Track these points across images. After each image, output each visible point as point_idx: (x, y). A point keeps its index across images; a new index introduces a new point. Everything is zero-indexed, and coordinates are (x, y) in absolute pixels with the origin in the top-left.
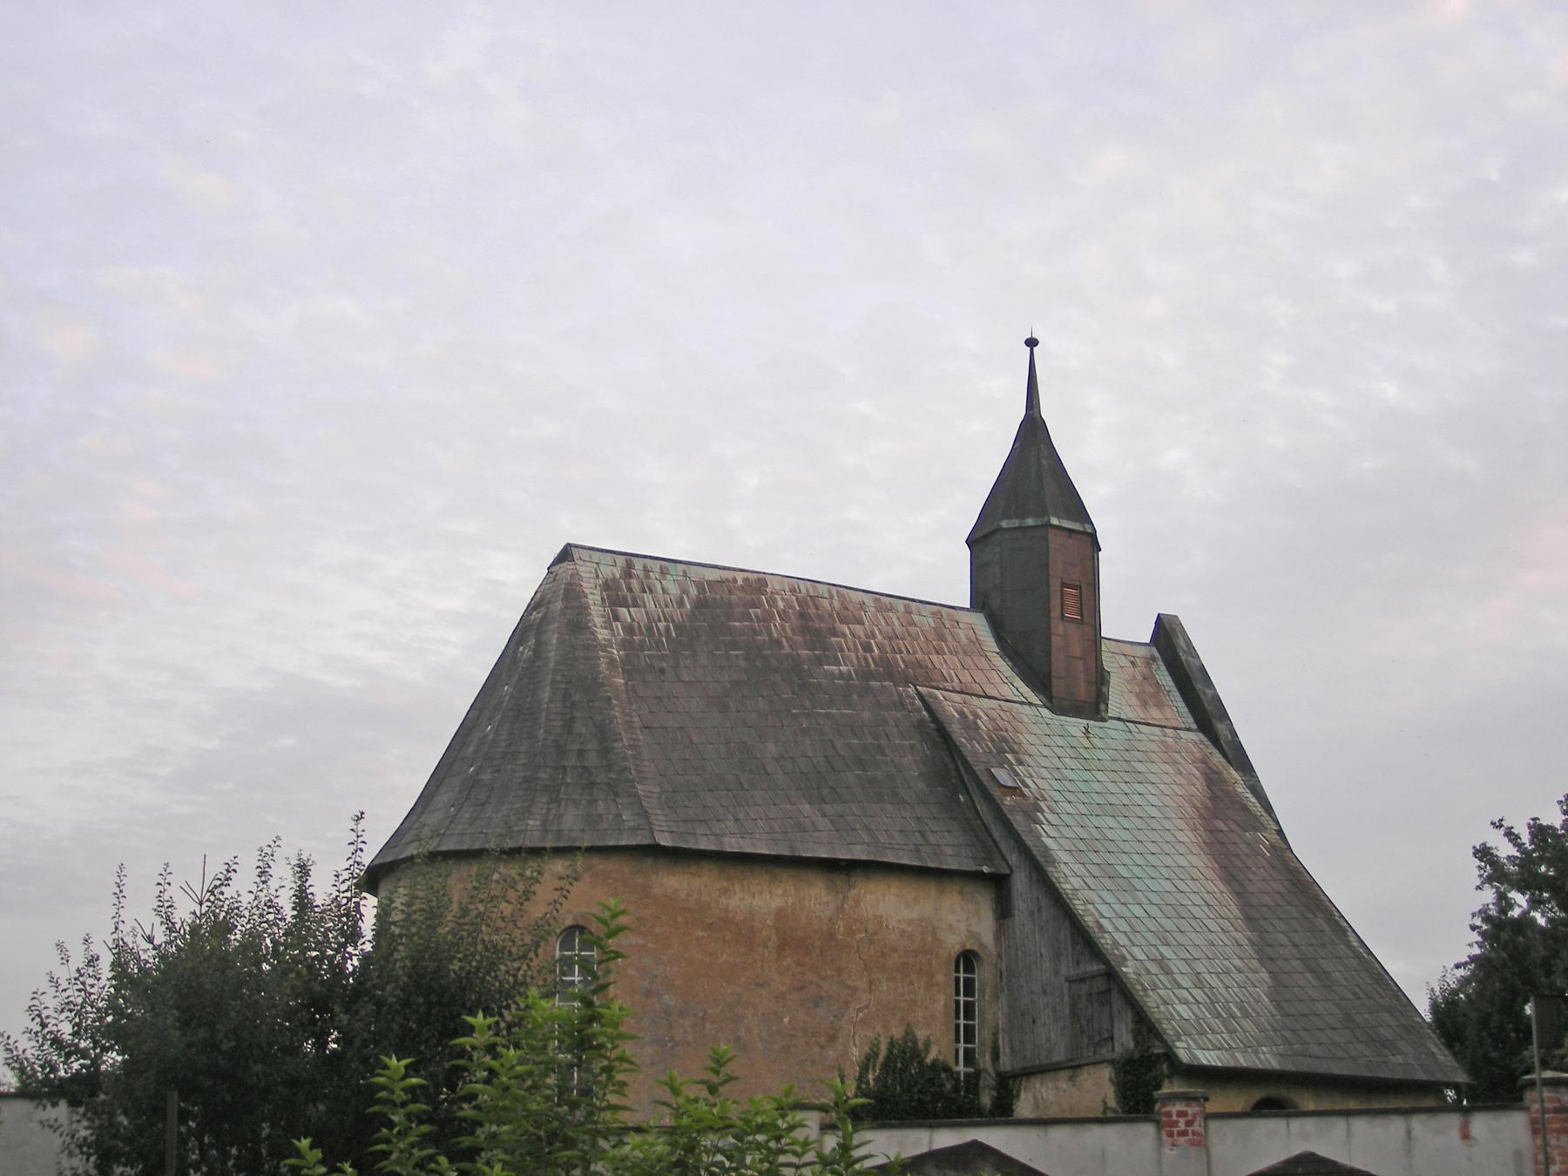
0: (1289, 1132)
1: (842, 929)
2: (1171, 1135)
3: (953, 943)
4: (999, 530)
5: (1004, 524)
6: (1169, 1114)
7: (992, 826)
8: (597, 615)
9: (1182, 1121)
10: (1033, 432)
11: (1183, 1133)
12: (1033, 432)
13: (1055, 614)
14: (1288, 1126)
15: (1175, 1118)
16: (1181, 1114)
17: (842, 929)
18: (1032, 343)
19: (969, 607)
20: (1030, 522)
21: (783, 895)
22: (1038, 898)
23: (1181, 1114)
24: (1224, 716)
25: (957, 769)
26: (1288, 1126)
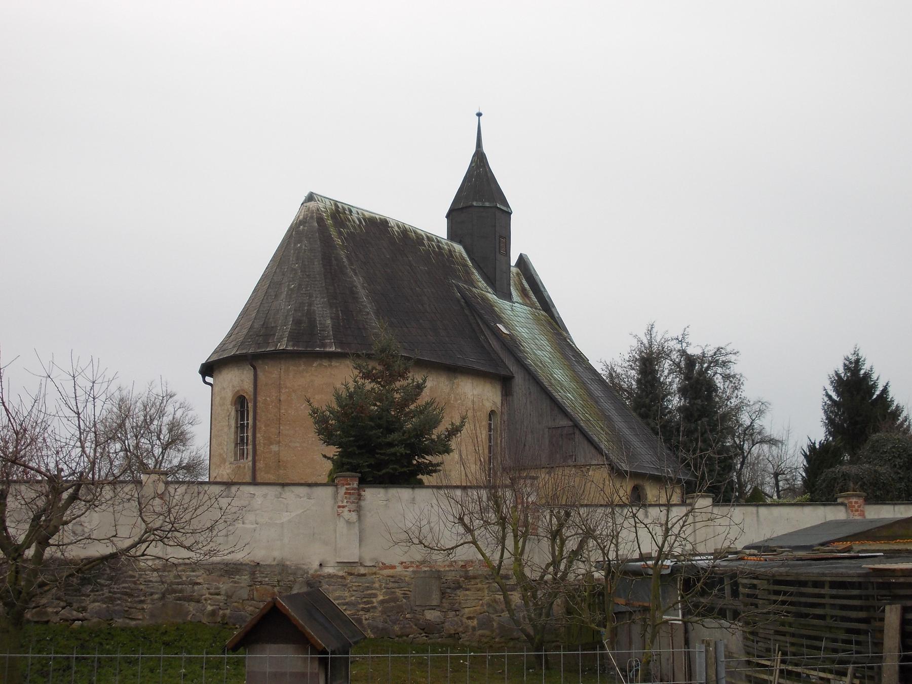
0: (895, 511)
1: (453, 398)
2: (852, 511)
3: (489, 406)
4: (472, 206)
5: (475, 204)
6: (851, 502)
7: (500, 352)
8: (333, 233)
9: (856, 505)
10: (480, 159)
11: (857, 511)
12: (480, 159)
13: (497, 250)
14: (894, 509)
15: (853, 504)
16: (856, 503)
17: (453, 398)
18: (479, 115)
19: (446, 238)
20: (487, 204)
21: (433, 380)
22: (529, 388)
23: (856, 503)
24: (554, 306)
25: (478, 323)
26: (894, 509)
